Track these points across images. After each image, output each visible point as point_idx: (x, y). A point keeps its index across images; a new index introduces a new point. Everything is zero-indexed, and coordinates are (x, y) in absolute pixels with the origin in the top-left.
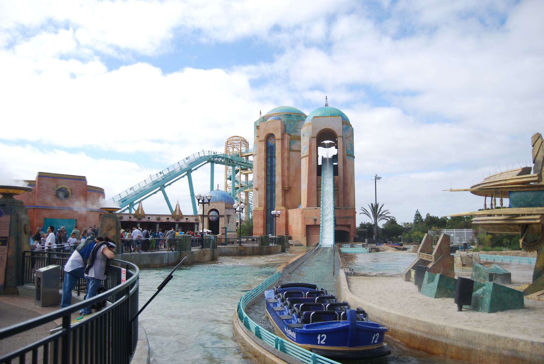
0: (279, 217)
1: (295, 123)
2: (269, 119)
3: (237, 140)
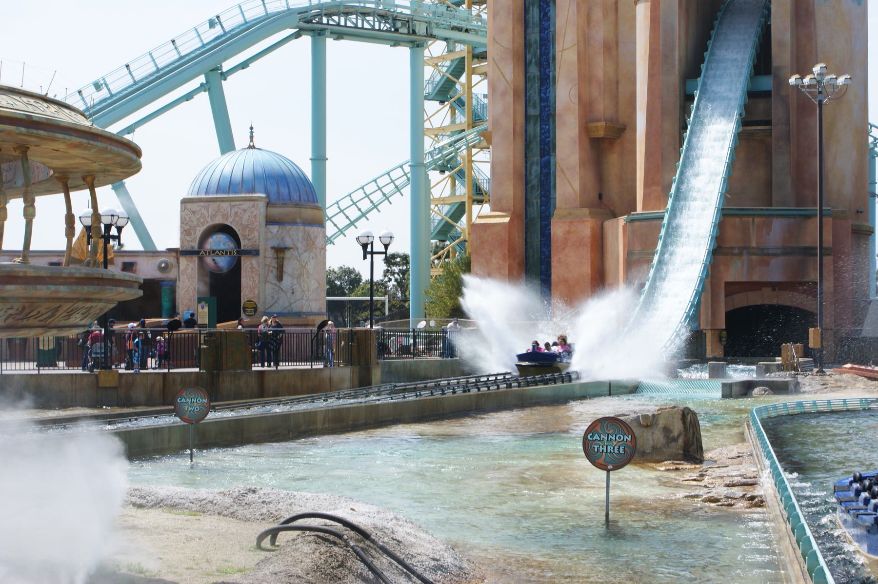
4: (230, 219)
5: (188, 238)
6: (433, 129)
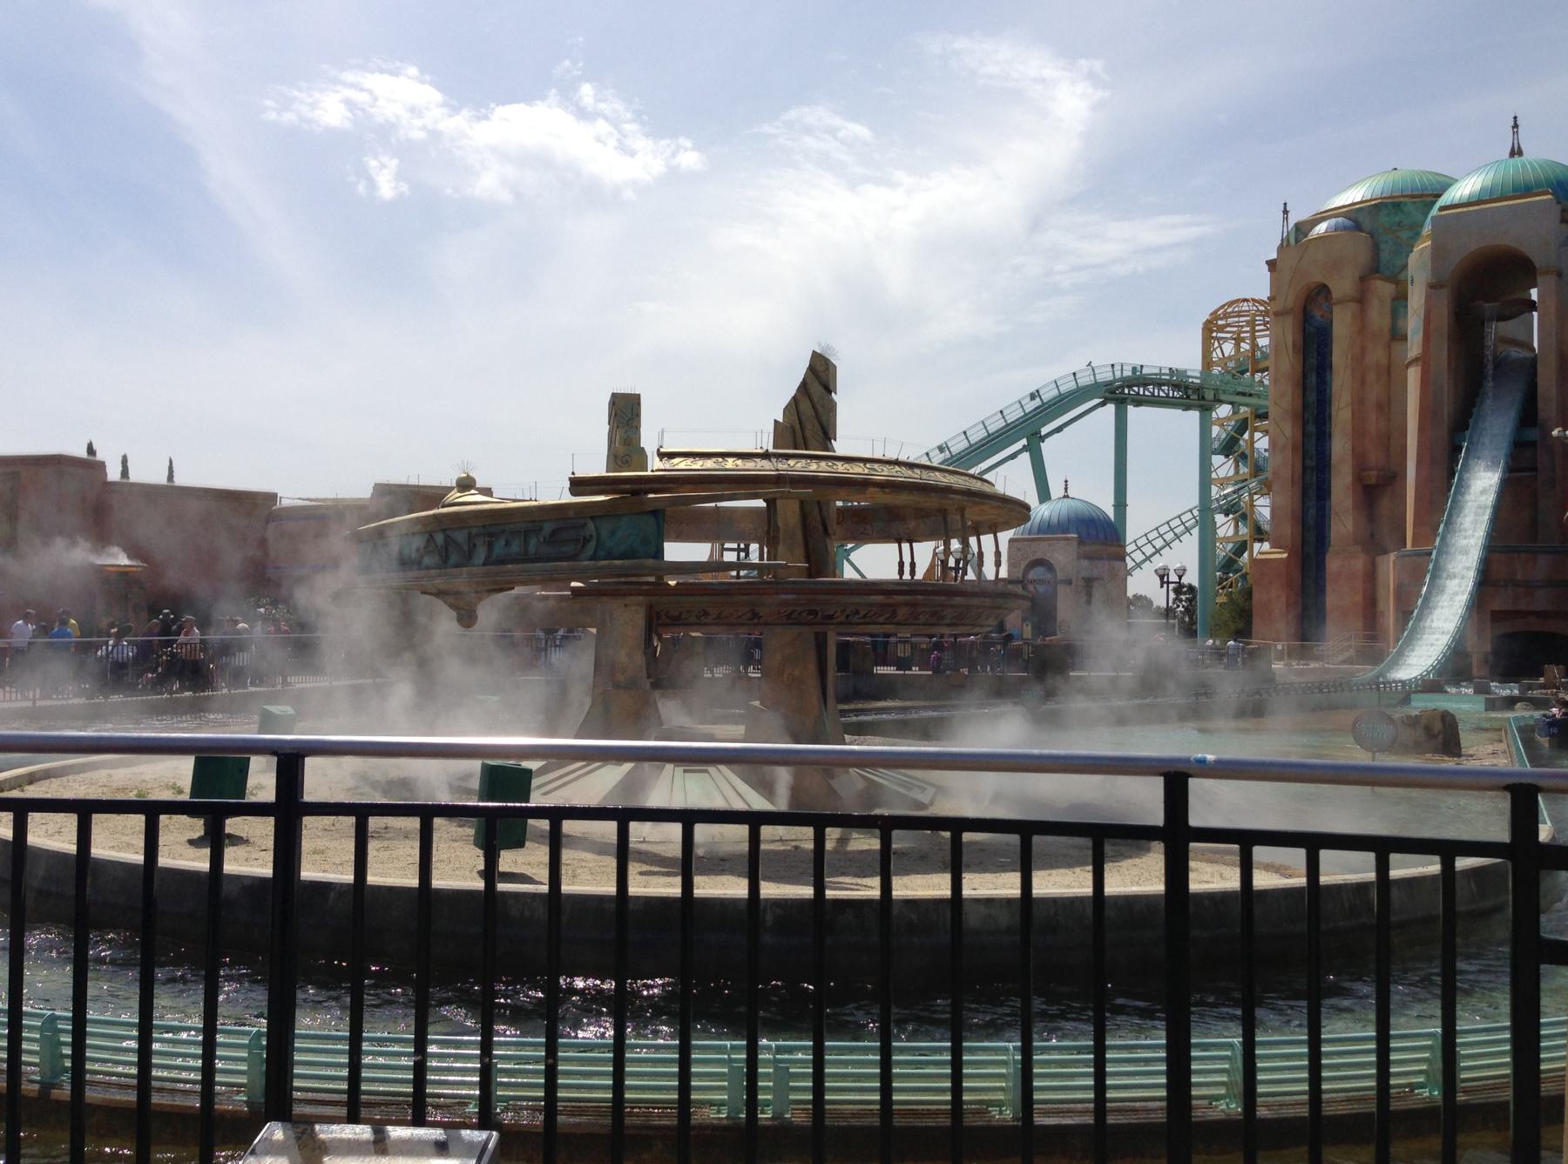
2: (1321, 228)
5: (1014, 570)
6: (1219, 478)
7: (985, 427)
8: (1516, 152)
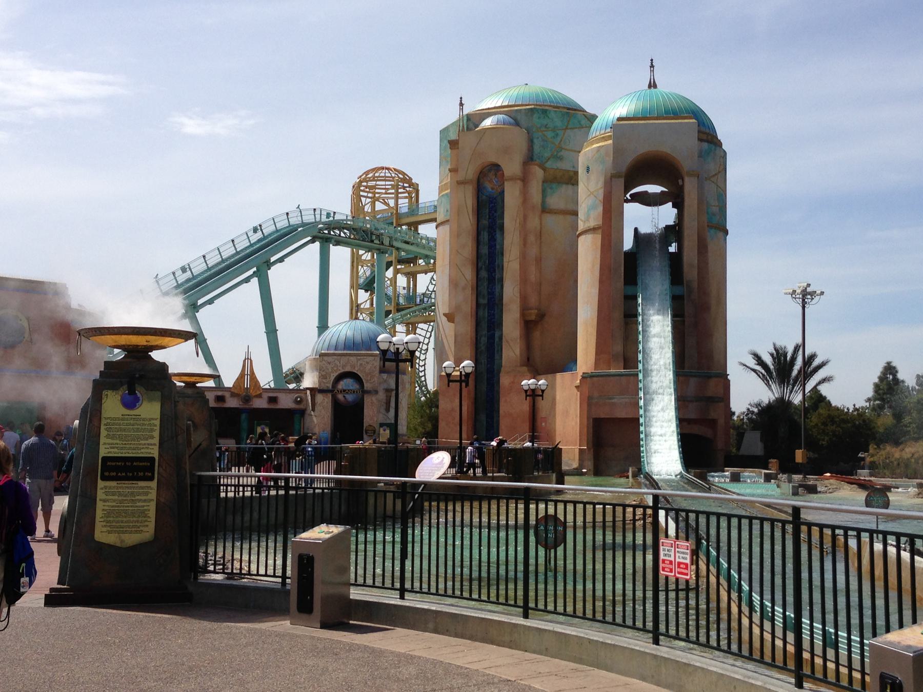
0: (542, 396)
1: (557, 135)
2: (488, 123)
3: (385, 179)
4: (356, 369)
5: (324, 380)
7: (220, 253)
8: (652, 85)
